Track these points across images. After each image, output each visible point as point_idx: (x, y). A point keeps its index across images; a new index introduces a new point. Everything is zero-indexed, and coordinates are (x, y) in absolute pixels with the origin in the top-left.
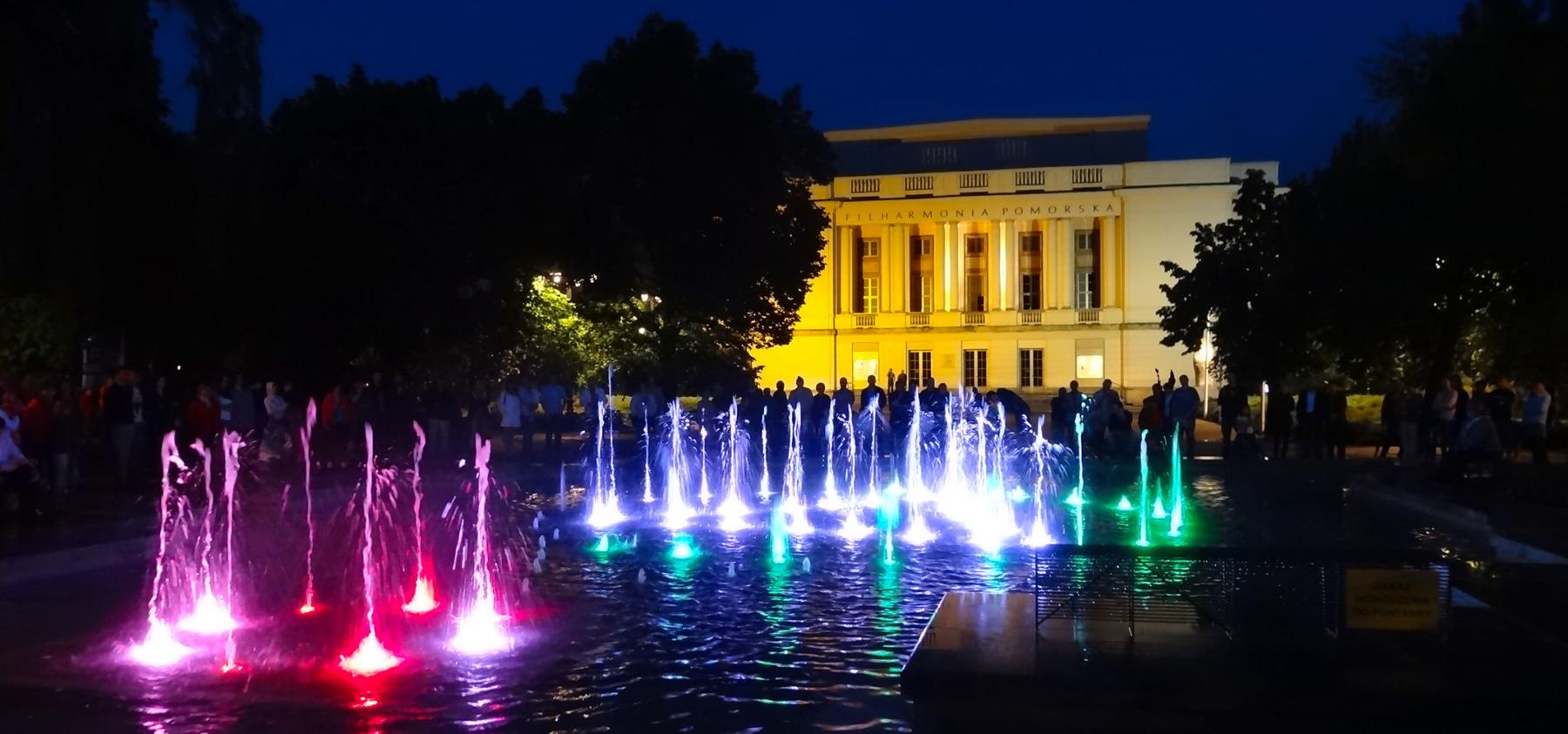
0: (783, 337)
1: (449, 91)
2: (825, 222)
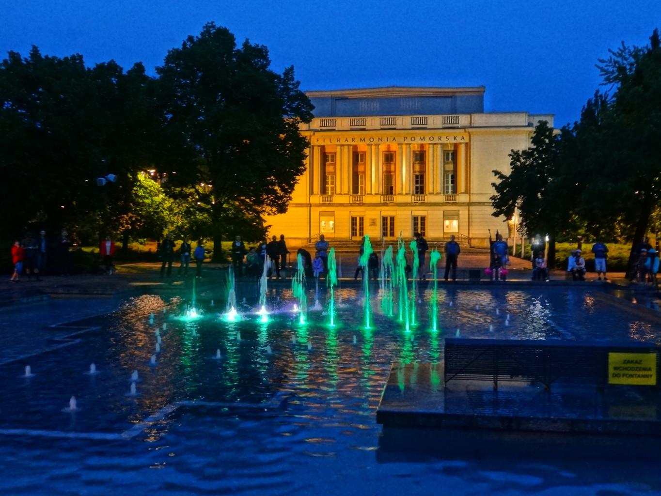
0: (282, 209)
1: (89, 64)
2: (307, 145)
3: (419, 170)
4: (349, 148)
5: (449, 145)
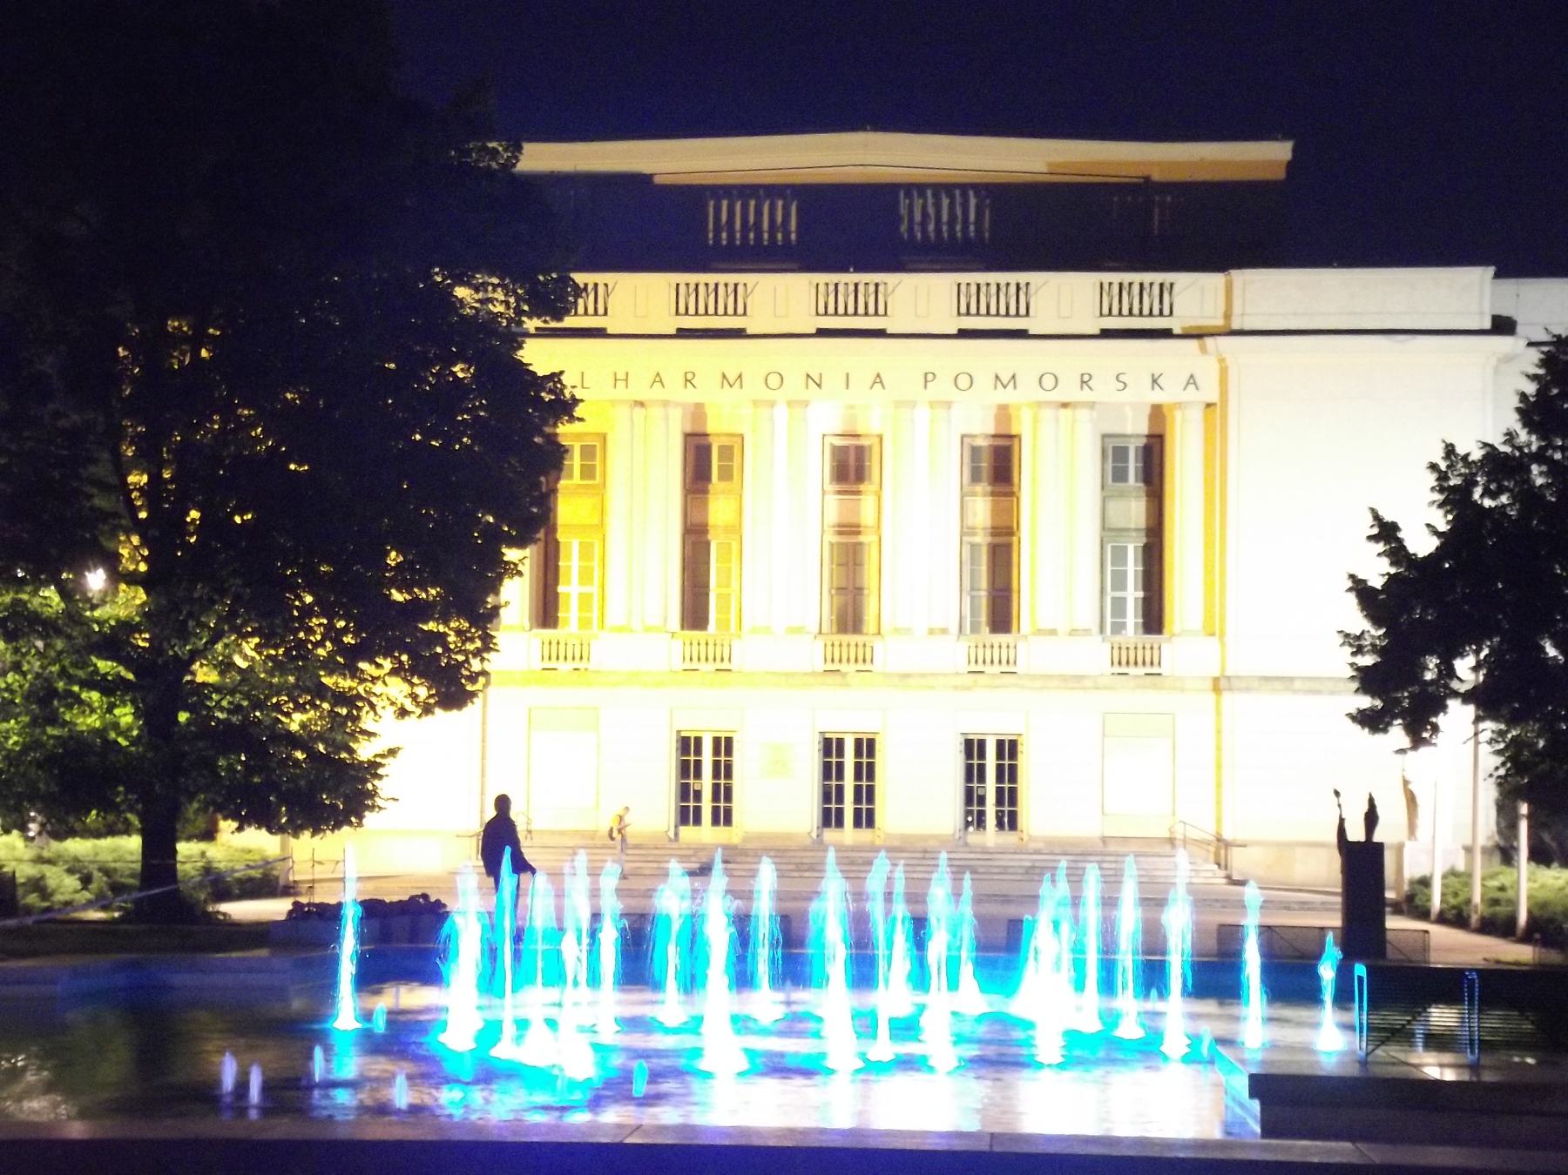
3: (988, 523)
4: (667, 418)
5: (1128, 410)
